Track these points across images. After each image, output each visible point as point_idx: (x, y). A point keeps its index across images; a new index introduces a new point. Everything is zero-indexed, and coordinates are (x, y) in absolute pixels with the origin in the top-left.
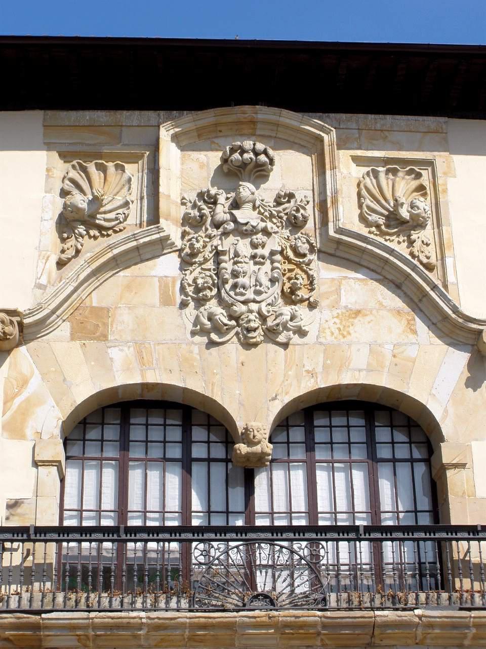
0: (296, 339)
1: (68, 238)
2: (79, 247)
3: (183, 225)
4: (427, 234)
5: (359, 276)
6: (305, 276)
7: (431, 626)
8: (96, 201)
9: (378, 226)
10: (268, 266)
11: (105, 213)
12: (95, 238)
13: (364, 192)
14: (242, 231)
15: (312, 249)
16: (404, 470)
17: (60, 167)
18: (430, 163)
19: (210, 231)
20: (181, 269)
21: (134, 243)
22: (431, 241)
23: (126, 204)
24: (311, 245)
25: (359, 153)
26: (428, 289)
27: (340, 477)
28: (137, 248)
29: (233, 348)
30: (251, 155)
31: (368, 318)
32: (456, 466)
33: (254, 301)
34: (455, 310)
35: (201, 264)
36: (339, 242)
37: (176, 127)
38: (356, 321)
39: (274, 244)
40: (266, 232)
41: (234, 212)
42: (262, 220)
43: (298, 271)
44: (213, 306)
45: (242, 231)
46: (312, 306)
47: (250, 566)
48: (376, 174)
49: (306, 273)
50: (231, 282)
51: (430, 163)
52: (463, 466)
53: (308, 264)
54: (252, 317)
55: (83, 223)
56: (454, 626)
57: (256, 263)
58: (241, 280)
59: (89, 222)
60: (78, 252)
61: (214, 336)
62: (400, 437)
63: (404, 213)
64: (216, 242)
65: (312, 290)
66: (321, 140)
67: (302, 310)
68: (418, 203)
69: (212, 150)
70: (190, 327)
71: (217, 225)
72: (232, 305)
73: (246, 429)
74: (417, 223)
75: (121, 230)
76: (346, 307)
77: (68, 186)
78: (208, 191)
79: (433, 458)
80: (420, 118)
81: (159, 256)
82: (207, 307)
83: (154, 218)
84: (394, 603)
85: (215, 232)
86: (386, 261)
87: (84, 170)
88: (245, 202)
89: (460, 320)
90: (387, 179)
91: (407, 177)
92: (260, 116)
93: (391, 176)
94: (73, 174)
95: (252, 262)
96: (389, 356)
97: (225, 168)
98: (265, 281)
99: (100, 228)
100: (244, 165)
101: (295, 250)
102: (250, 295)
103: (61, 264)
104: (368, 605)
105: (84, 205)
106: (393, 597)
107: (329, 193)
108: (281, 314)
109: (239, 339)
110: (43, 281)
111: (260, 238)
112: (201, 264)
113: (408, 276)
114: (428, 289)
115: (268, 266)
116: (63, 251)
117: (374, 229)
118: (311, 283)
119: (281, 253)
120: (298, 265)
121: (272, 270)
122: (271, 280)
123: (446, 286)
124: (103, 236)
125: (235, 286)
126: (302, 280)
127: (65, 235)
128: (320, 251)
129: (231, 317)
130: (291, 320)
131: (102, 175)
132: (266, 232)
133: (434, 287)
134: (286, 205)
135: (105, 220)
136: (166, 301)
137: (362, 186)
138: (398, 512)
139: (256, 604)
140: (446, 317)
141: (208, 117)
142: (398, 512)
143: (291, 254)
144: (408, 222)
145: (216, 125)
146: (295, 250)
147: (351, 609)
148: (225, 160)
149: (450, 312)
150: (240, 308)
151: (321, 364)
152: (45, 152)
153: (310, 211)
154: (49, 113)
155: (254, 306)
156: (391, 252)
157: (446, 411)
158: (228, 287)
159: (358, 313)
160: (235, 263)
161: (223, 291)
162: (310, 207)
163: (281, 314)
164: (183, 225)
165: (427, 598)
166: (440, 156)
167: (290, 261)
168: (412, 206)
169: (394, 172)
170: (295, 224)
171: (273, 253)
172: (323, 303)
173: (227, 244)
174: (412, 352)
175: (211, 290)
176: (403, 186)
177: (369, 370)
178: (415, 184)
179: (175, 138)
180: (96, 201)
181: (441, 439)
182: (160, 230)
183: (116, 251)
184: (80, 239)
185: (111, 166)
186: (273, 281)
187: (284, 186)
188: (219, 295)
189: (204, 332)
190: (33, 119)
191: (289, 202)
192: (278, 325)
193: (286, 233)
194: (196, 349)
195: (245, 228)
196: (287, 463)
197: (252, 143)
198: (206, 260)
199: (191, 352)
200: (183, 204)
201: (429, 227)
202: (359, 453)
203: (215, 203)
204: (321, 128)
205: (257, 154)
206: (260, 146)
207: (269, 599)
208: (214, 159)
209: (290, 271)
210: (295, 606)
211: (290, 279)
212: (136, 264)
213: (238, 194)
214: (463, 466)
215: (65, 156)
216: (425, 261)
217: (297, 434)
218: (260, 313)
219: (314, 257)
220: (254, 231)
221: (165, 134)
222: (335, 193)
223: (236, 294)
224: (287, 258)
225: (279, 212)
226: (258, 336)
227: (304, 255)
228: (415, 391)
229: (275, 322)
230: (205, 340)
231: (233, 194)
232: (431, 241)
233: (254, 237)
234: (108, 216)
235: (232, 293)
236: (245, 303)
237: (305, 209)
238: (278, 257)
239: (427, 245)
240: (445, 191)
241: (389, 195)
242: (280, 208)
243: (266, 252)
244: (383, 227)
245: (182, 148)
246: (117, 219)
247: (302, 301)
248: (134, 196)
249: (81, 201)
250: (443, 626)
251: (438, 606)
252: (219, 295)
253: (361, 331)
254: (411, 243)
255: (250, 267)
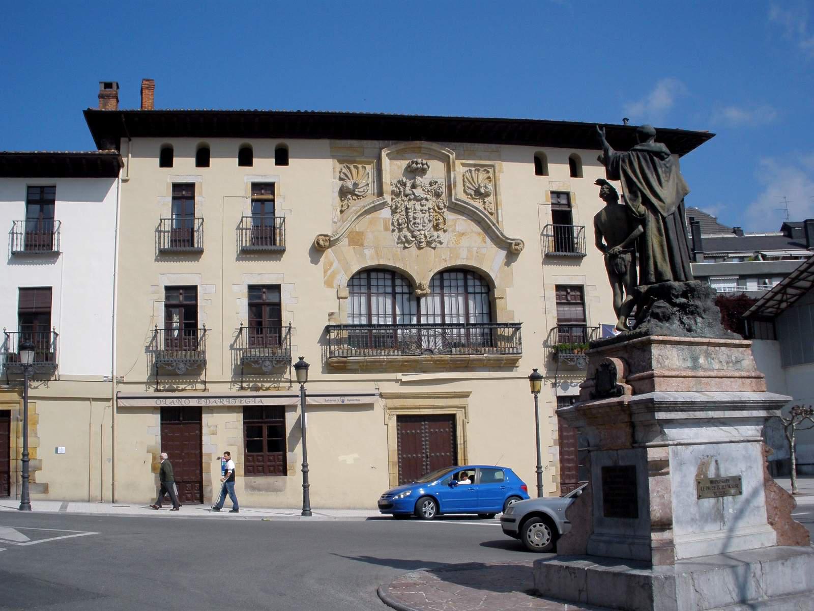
0: (438, 245)
1: (344, 200)
2: (349, 204)
3: (392, 194)
4: (490, 199)
5: (464, 218)
6: (442, 218)
7: (489, 360)
8: (356, 185)
9: (471, 195)
10: (427, 215)
11: (359, 188)
12: (355, 200)
13: (466, 180)
14: (417, 199)
15: (445, 206)
16: (478, 297)
17: (339, 166)
18: (493, 166)
19: (403, 198)
20: (392, 215)
21: (373, 205)
22: (493, 202)
23: (368, 185)
24: (444, 205)
25: (464, 161)
26: (491, 225)
27: (453, 299)
28: (374, 206)
29: (413, 248)
30: (421, 165)
31: (467, 237)
32: (500, 298)
33: (422, 230)
34: (502, 234)
35: (400, 213)
36: (456, 204)
37: (389, 150)
38: (462, 238)
39: (430, 205)
40: (426, 199)
41: (413, 190)
42: (426, 194)
43: (439, 216)
44: (405, 232)
45: (417, 199)
46: (445, 231)
47: (420, 337)
48: (470, 171)
49: (443, 217)
50: (413, 221)
51: (493, 166)
52: (502, 298)
53: (443, 213)
54: (422, 237)
55: (350, 193)
56: (498, 360)
57: (422, 213)
58: (416, 221)
59: (353, 193)
60: (348, 206)
61: (406, 245)
62: (477, 283)
63: (482, 190)
64: (406, 203)
65: (445, 224)
66: (449, 157)
67: (441, 233)
68: (488, 187)
69: (402, 160)
70: (396, 240)
71: (406, 196)
72: (414, 231)
73: (420, 284)
74: (487, 195)
75: (366, 197)
76: (458, 231)
77: (343, 176)
78: (402, 180)
79: (490, 293)
80: (490, 145)
81: (382, 209)
82: (404, 232)
83: (380, 193)
84: (476, 352)
85: (405, 199)
86: (475, 212)
87: (349, 168)
88: (418, 186)
89: (504, 239)
90: (475, 173)
91: (483, 172)
92: (423, 146)
93: (477, 172)
94: (344, 170)
95: (421, 212)
96: (475, 253)
97: (409, 169)
98: (427, 221)
99: (357, 195)
100: (417, 169)
101: (438, 207)
102: (420, 227)
103: (342, 212)
104: (467, 353)
105: (351, 187)
106: (476, 349)
107: (452, 182)
108: (433, 236)
109: (416, 246)
110: (336, 220)
111: (424, 202)
112: (400, 213)
113: (484, 219)
114: (491, 225)
115: (427, 215)
116: (342, 206)
117: (469, 196)
118: (445, 222)
119: (433, 208)
120: (439, 213)
121: (430, 216)
122: (429, 220)
123: (498, 222)
124: (358, 199)
125: (414, 223)
126: (441, 221)
127: (343, 199)
128: (448, 207)
129: (413, 237)
130: (437, 238)
131: (356, 170)
132: (426, 199)
133: (494, 225)
134: (435, 186)
135: (359, 192)
136: (386, 229)
137: (465, 177)
138: (476, 314)
139: (426, 352)
140: (498, 237)
141: (402, 145)
142: (476, 314)
143: (436, 208)
144: (483, 194)
145: (404, 149)
146: (438, 207)
147: (460, 354)
148: (409, 166)
149: (500, 235)
150: (417, 233)
151: (448, 256)
152: (331, 160)
153: (444, 190)
154: (333, 141)
155: (422, 232)
156: (477, 209)
157: (497, 276)
158: (411, 223)
159: (463, 234)
160: (415, 213)
161: (409, 225)
162: (443, 187)
163: (433, 236)
164: (392, 194)
165: (489, 350)
166: (497, 163)
167: (436, 212)
168: (486, 187)
169: (478, 170)
170: (438, 195)
171: (429, 209)
172: (450, 230)
173: (410, 205)
174: (484, 251)
175: (404, 224)
176: (482, 176)
177: (467, 259)
178: (486, 176)
179: (388, 155)
180: (356, 185)
181: (494, 287)
182: (384, 199)
183: (366, 208)
184: (350, 201)
185: (360, 166)
186: (430, 221)
187: (432, 178)
188: (408, 226)
189: (402, 243)
190: (325, 143)
191: (435, 184)
192: (432, 240)
193: (434, 199)
194: (399, 249)
195: (418, 198)
196: (433, 294)
197: (421, 160)
198: (402, 211)
199: (397, 251)
200: (391, 185)
201: (492, 195)
202: (461, 290)
203: (405, 185)
204: (449, 152)
205: (423, 164)
206: (424, 162)
207: (430, 351)
208: (404, 163)
209: (436, 216)
210: (440, 353)
211: (436, 220)
212: (373, 212)
213: (415, 182)
214: (502, 298)
215: (340, 162)
216: (490, 211)
217: (437, 283)
218: (425, 235)
219: (445, 210)
220: (422, 199)
221: (384, 153)
222: (455, 182)
223: (415, 227)
224: (434, 210)
225: (431, 190)
226: (423, 245)
227: (442, 209)
228: (485, 268)
229: (431, 239)
230: (403, 246)
231: (412, 181)
232: (493, 202)
233: (422, 202)
234: (360, 190)
235: (413, 226)
236: (419, 230)
237: (442, 188)
238: (432, 210)
239: (491, 203)
240: (499, 179)
241: (475, 180)
242: (432, 188)
243: (426, 208)
244: (473, 196)
245: (390, 159)
246: (364, 191)
247: (441, 229)
248: (370, 181)
249: (349, 184)
250: (494, 360)
251: (493, 353)
252: (408, 226)
253: (464, 242)
254: (484, 203)
255: (420, 215)
